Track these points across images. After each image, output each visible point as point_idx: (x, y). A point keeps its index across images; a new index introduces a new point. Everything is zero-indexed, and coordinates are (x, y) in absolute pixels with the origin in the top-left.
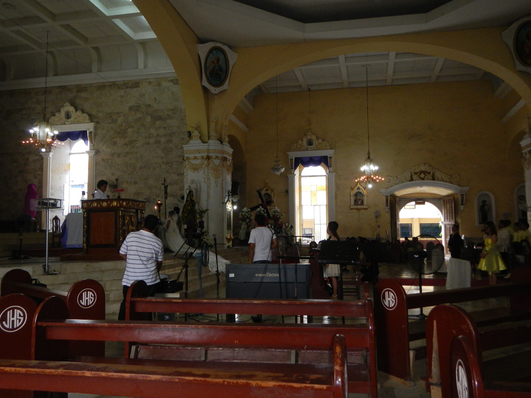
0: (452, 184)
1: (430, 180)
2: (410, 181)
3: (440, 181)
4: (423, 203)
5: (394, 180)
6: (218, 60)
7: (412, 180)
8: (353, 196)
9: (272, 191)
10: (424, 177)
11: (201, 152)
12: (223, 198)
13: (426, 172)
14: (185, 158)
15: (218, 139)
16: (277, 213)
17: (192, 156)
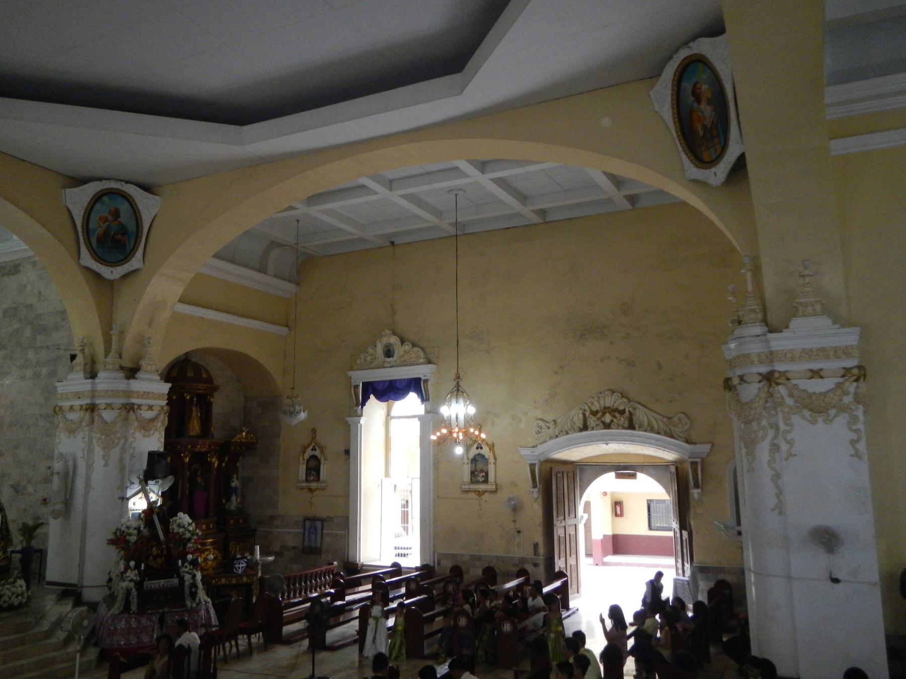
0: (672, 437)
1: (624, 428)
2: (581, 430)
3: (646, 431)
4: (633, 476)
5: (549, 428)
6: (116, 214)
7: (585, 428)
8: (468, 464)
9: (322, 452)
10: (612, 421)
11: (81, 396)
12: (123, 488)
13: (616, 410)
14: (57, 409)
15: (122, 368)
16: (181, 530)
17: (66, 404)
